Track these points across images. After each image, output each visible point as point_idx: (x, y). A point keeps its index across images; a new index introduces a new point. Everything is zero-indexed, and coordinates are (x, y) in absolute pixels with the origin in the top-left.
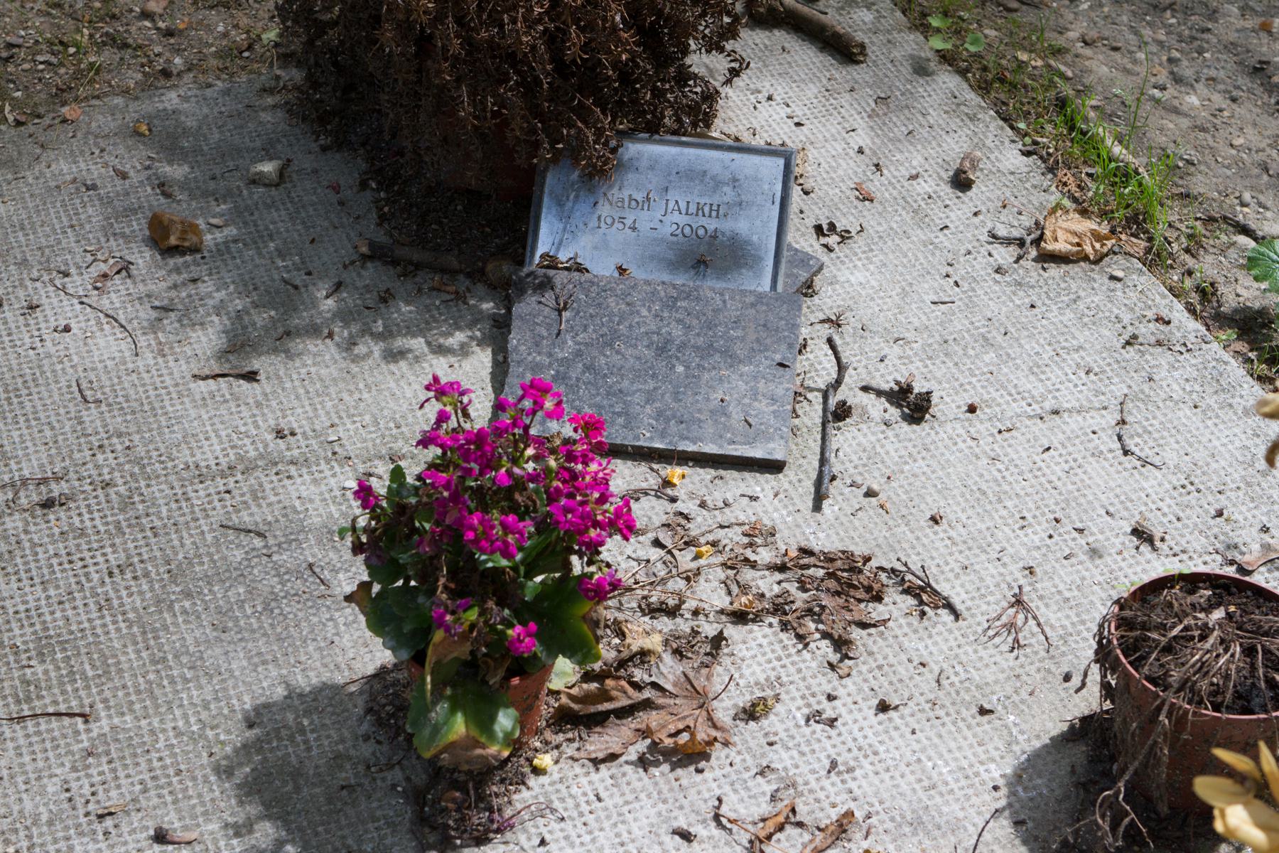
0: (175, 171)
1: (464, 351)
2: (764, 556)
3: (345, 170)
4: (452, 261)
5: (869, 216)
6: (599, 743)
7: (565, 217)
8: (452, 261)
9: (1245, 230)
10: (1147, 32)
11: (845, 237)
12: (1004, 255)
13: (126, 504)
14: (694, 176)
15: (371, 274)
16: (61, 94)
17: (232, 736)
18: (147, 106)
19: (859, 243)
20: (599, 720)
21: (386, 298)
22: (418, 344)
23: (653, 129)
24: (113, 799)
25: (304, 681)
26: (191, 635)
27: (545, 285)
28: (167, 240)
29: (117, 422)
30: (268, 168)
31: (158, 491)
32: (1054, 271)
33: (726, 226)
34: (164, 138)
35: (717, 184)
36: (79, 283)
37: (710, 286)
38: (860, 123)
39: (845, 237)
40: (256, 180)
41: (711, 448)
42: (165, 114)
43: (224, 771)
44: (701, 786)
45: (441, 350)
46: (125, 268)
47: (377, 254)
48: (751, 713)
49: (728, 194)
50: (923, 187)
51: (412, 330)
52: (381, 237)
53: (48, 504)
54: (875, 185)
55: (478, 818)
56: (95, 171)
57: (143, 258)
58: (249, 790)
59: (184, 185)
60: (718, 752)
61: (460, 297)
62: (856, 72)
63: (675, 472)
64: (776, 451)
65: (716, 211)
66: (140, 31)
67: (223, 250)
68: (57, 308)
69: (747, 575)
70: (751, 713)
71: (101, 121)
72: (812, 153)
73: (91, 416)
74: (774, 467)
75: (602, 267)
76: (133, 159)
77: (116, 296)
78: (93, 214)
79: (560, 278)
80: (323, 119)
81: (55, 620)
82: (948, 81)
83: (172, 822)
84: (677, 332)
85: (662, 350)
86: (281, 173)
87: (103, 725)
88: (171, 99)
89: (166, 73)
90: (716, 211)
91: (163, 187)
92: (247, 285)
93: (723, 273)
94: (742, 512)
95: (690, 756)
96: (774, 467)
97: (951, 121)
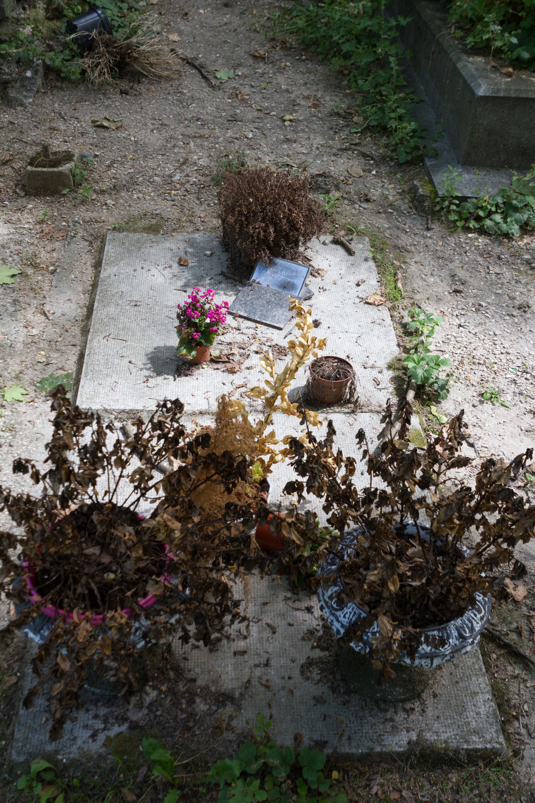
0: (190, 250)
1: (231, 295)
2: (269, 344)
3: (225, 257)
4: (237, 278)
5: (333, 288)
6: (216, 366)
7: (260, 273)
8: (237, 278)
9: (420, 307)
10: (432, 263)
11: (325, 290)
12: (358, 300)
13: (150, 308)
14: (288, 269)
15: (220, 278)
16: (174, 230)
17: (151, 350)
18: (191, 236)
19: (327, 292)
20: (217, 362)
21: (220, 283)
22: (222, 292)
23: (284, 257)
24: (123, 354)
25: (168, 344)
26: (151, 333)
27: (251, 285)
28: (182, 263)
29: (155, 294)
30: (208, 253)
31: (157, 308)
32: (367, 306)
33: (292, 281)
34: (191, 243)
35: (293, 271)
36: (160, 268)
37: (284, 292)
38: (344, 268)
39: (325, 290)
40: (205, 255)
41: (268, 323)
42: (193, 238)
43: (147, 355)
44: (231, 377)
45: (226, 294)
46: (170, 267)
47: (222, 274)
48: (248, 368)
49: (294, 274)
50: (349, 284)
51: (222, 289)
52: (225, 270)
53: (136, 305)
54: (339, 282)
55: (189, 373)
56: (173, 247)
57: (175, 265)
58: (149, 359)
59: (191, 253)
60: (238, 373)
61: (235, 285)
62: (351, 258)
63: (259, 325)
64: (281, 326)
65: (291, 277)
66: (197, 220)
67: (192, 267)
68: (154, 271)
69: (263, 346)
70: (248, 368)
71: (180, 237)
72: (329, 272)
73: (151, 292)
74: (280, 329)
75: (264, 285)
76: (182, 246)
77: (167, 272)
78: (169, 255)
79: (254, 284)
80: (225, 245)
81: (128, 325)
82: (371, 263)
83: (133, 361)
84: (273, 299)
85: (268, 302)
86: (211, 254)
87: (128, 343)
88: (196, 235)
89: (198, 230)
90: (291, 277)
91: (186, 253)
92: (193, 275)
93: (289, 290)
94: (269, 336)
95: (232, 371)
96: (280, 329)
97: (369, 274)
